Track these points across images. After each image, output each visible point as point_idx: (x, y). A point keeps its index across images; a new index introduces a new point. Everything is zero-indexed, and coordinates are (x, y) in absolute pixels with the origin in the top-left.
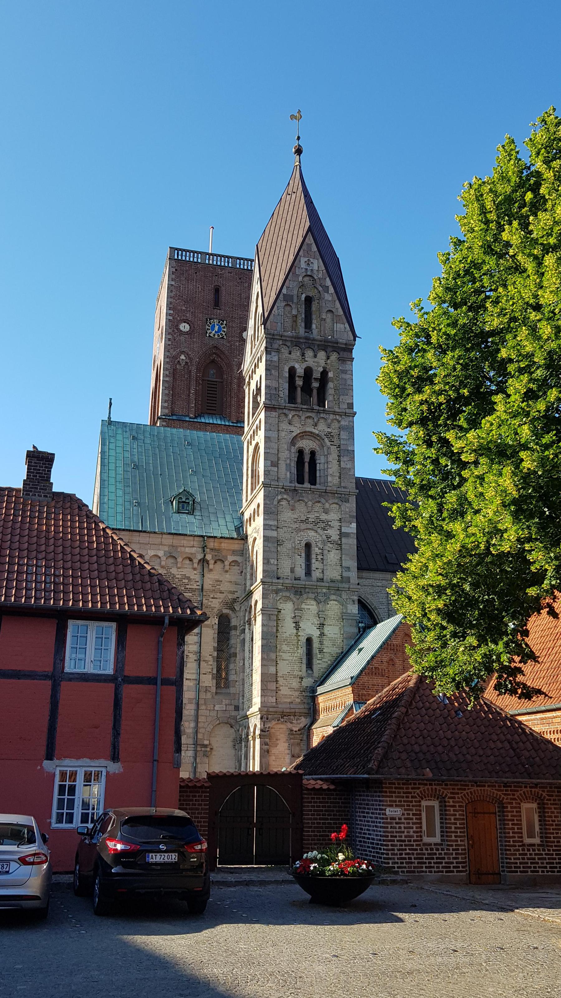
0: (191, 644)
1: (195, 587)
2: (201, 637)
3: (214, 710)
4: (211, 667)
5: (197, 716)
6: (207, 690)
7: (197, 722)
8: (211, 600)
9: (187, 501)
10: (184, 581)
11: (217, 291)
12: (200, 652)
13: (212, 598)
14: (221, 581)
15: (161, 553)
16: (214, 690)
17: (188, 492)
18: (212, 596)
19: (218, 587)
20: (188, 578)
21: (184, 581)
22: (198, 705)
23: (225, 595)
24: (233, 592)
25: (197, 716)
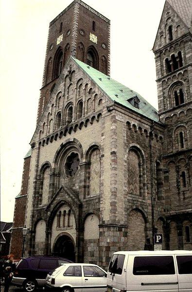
5: (153, 213)
11: (94, 23)
25: (153, 213)
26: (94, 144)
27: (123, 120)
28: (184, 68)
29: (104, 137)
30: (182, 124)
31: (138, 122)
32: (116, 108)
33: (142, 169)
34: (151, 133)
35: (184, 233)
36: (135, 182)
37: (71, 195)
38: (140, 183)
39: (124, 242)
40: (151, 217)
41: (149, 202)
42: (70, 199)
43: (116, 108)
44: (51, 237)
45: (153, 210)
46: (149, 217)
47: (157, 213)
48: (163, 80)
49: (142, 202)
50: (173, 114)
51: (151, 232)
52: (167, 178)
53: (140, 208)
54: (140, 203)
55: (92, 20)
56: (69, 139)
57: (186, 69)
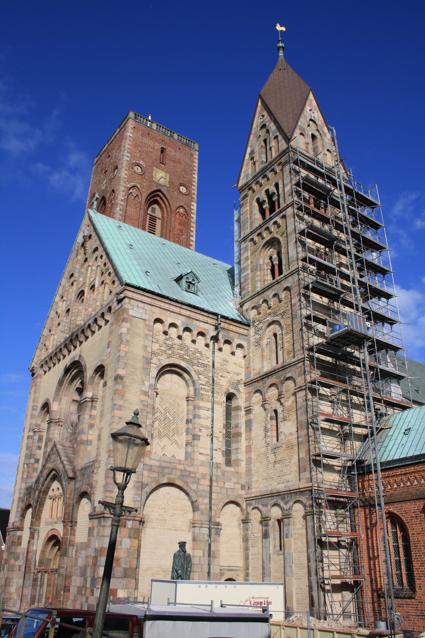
0: (203, 418)
1: (206, 362)
2: (213, 412)
3: (224, 487)
4: (221, 444)
6: (218, 466)
7: (211, 498)
8: (219, 377)
9: (193, 282)
10: (197, 355)
12: (212, 427)
13: (221, 376)
14: (228, 362)
15: (178, 323)
16: (223, 466)
17: (194, 275)
18: (220, 374)
19: (225, 366)
20: (200, 353)
21: (197, 355)
22: (211, 480)
23: (231, 375)
24: (238, 374)
26: (99, 364)
27: (145, 316)
28: (281, 212)
29: (109, 350)
30: (276, 318)
31: (183, 318)
32: (129, 294)
33: (191, 408)
34: (215, 339)
35: (274, 534)
36: (176, 432)
37: (63, 458)
38: (187, 434)
39: (128, 550)
40: (207, 501)
41: (205, 470)
42: (61, 466)
43: (129, 294)
44: (38, 539)
45: (211, 486)
46: (200, 500)
47: (224, 491)
48: (250, 238)
49: (185, 470)
50: (262, 301)
51: (205, 531)
52: (249, 423)
53: (178, 482)
54: (179, 473)
55: (158, 147)
56: (74, 357)
57: (284, 213)
